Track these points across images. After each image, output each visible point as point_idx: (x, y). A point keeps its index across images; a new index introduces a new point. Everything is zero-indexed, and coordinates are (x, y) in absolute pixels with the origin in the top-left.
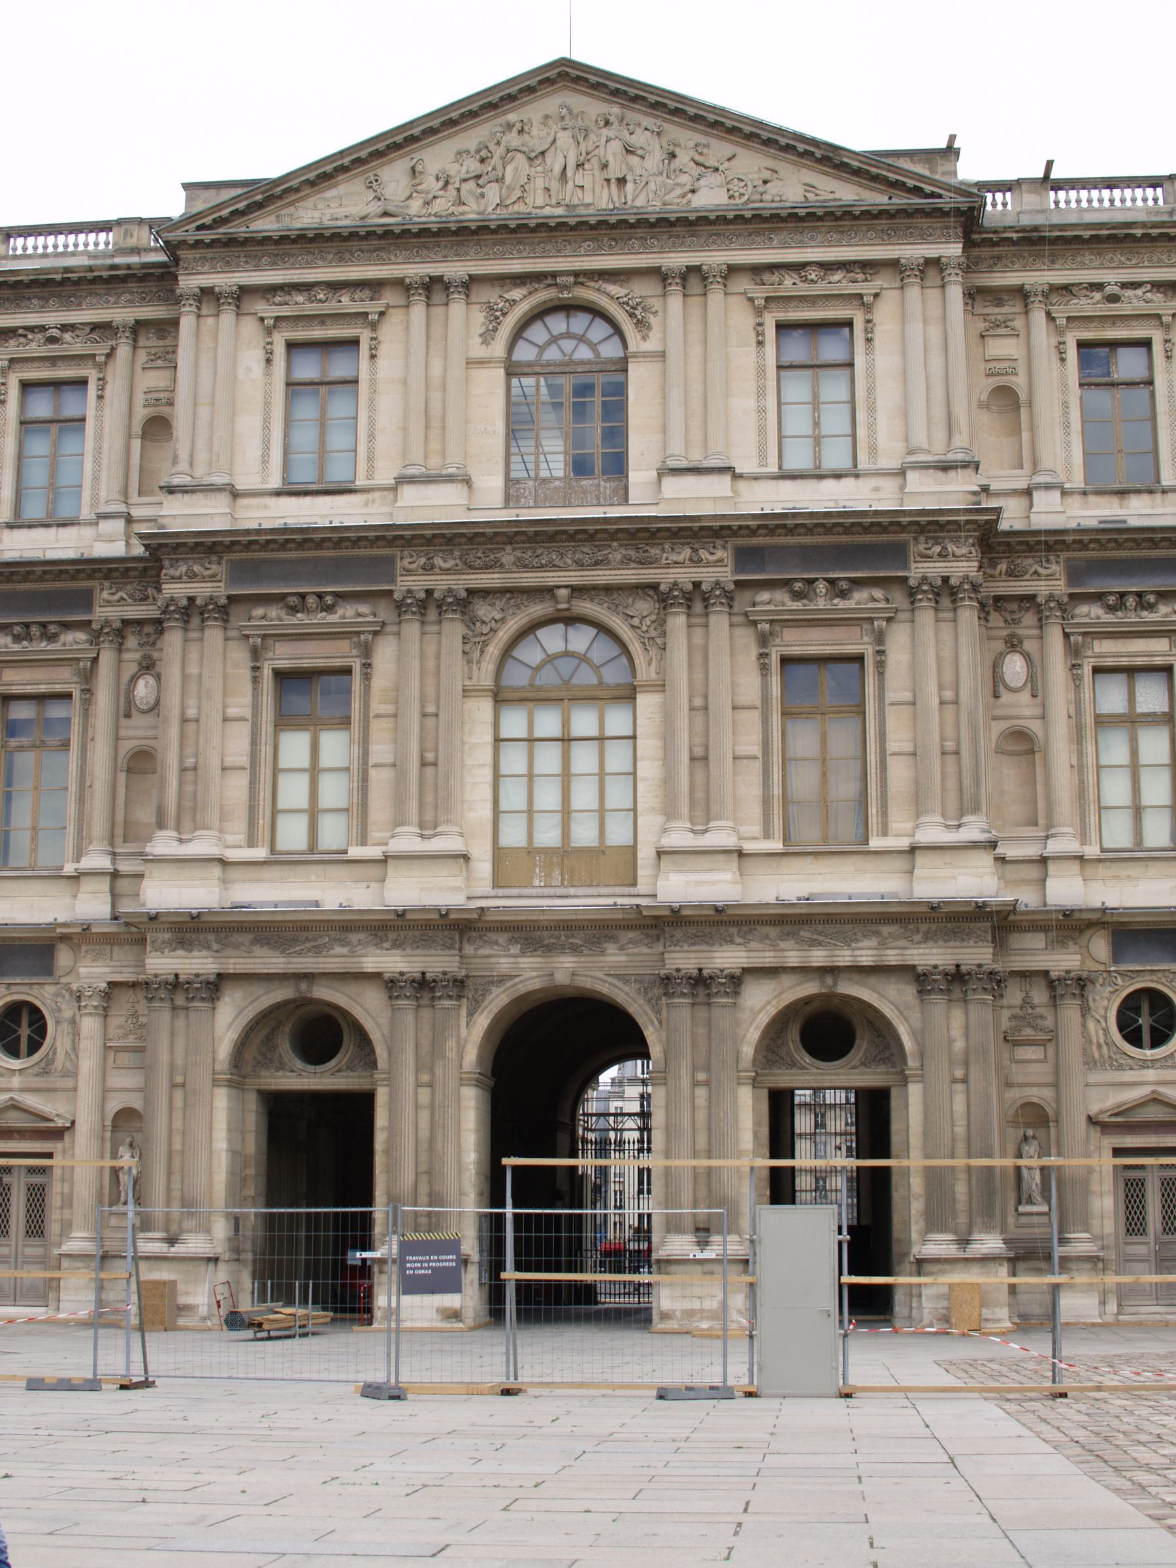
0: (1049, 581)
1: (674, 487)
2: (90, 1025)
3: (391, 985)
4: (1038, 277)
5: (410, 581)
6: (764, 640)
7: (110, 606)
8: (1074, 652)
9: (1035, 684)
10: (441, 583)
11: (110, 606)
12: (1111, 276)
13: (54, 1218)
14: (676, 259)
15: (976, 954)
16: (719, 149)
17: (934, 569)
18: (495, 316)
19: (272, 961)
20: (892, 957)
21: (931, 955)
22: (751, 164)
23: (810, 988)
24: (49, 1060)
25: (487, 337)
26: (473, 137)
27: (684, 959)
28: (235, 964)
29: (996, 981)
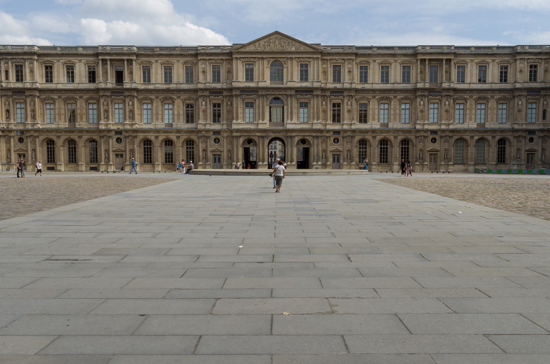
0: (328, 93)
1: (289, 83)
2: (225, 140)
3: (259, 137)
4: (329, 58)
5: (260, 93)
6: (298, 100)
7: (225, 93)
8: (330, 101)
9: (326, 104)
10: (264, 93)
11: (225, 93)
12: (337, 58)
13: (222, 160)
14: (289, 56)
15: (319, 134)
16: (294, 43)
17: (316, 93)
18: (269, 62)
19: (246, 134)
20: (310, 134)
21: (314, 134)
22: (298, 45)
23: (302, 137)
24: (220, 145)
25: (268, 64)
26: (266, 40)
27: (289, 134)
28: (242, 134)
29: (321, 137)
